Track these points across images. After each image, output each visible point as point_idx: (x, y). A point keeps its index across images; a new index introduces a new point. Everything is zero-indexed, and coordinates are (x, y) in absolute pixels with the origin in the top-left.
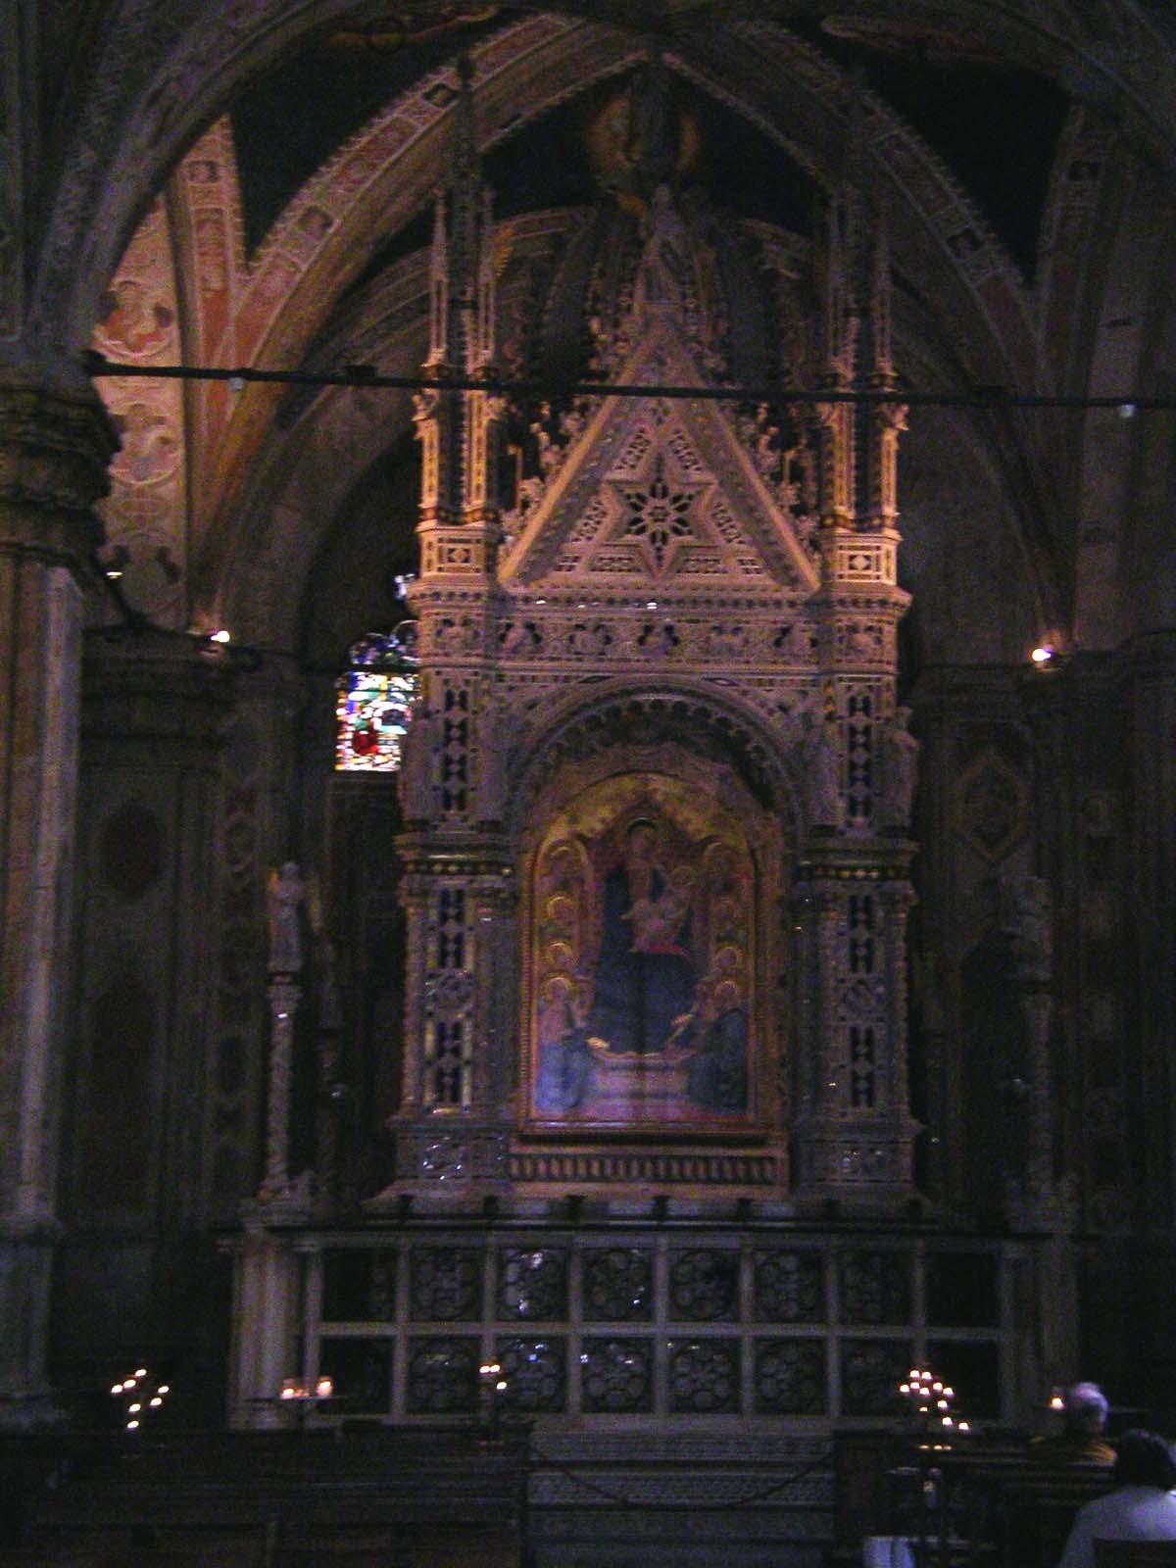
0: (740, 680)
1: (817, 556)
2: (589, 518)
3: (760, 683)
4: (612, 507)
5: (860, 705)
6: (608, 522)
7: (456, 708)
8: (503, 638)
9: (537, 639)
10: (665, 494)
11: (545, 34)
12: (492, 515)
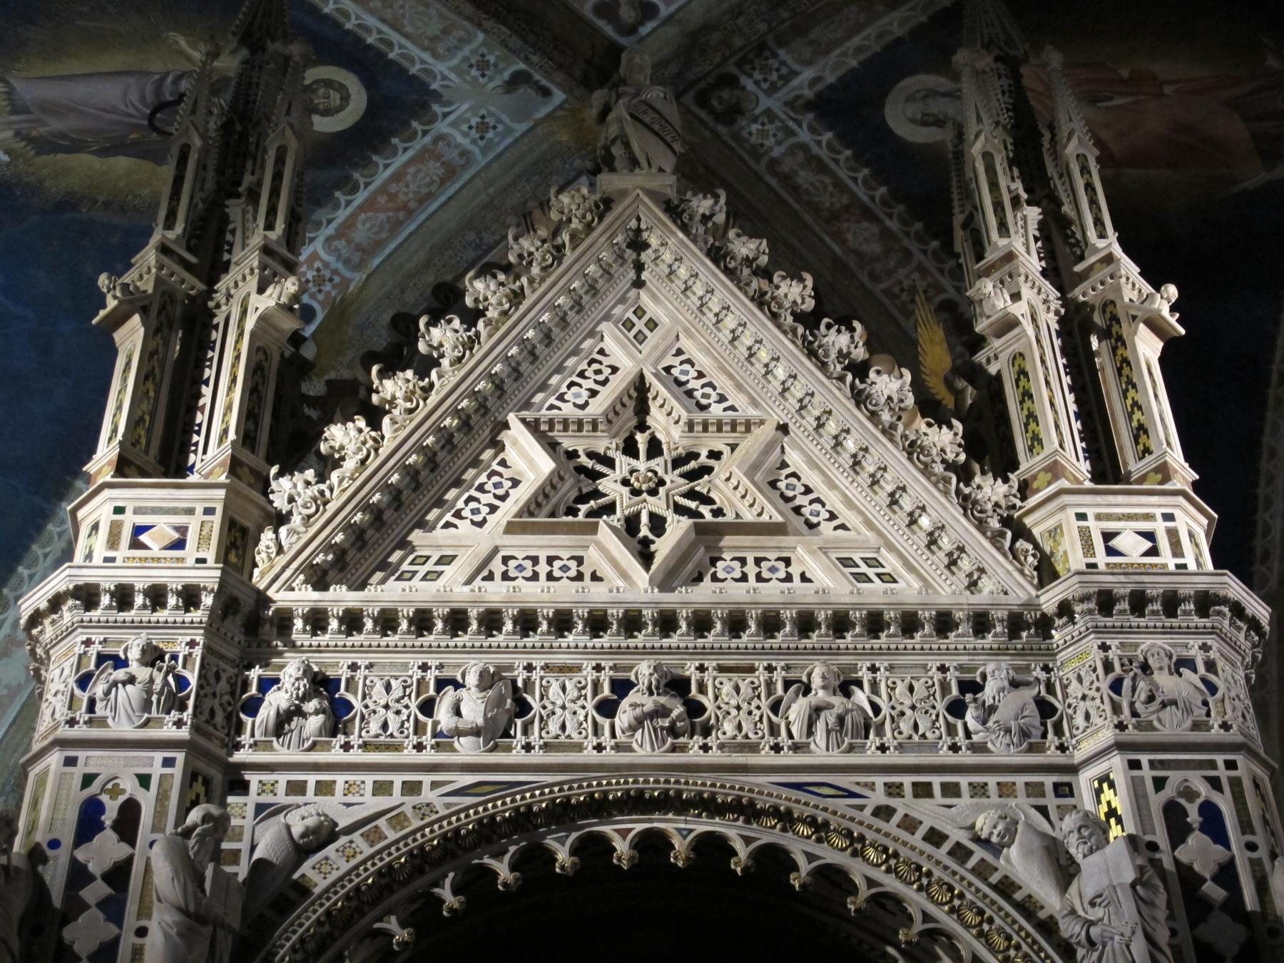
0: (871, 786)
1: (1021, 544)
2: (481, 488)
3: (923, 791)
4: (527, 460)
5: (1194, 816)
6: (520, 496)
8: (252, 707)
10: (655, 448)
11: (451, 173)
12: (248, 474)
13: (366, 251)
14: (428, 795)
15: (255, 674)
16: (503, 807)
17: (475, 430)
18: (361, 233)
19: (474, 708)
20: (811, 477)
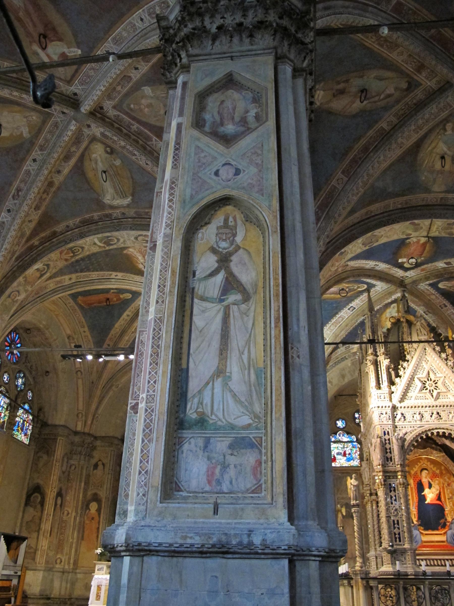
4: (418, 384)
7: (387, 435)
8: (396, 417)
9: (404, 417)
10: (431, 380)
13: (363, 301)
14: (415, 428)
15: (395, 413)
16: (423, 429)
17: (412, 379)
18: (363, 299)
19: (418, 417)
20: (448, 384)
